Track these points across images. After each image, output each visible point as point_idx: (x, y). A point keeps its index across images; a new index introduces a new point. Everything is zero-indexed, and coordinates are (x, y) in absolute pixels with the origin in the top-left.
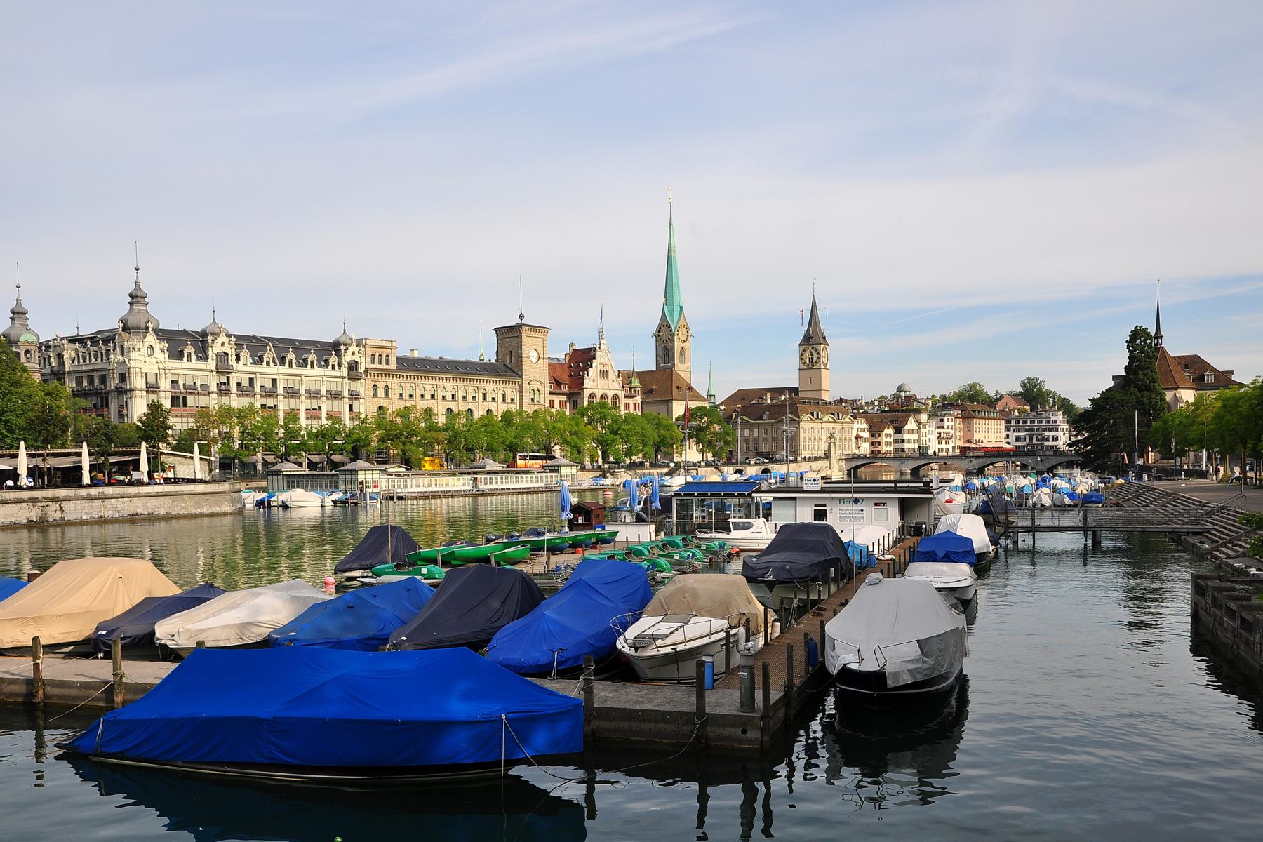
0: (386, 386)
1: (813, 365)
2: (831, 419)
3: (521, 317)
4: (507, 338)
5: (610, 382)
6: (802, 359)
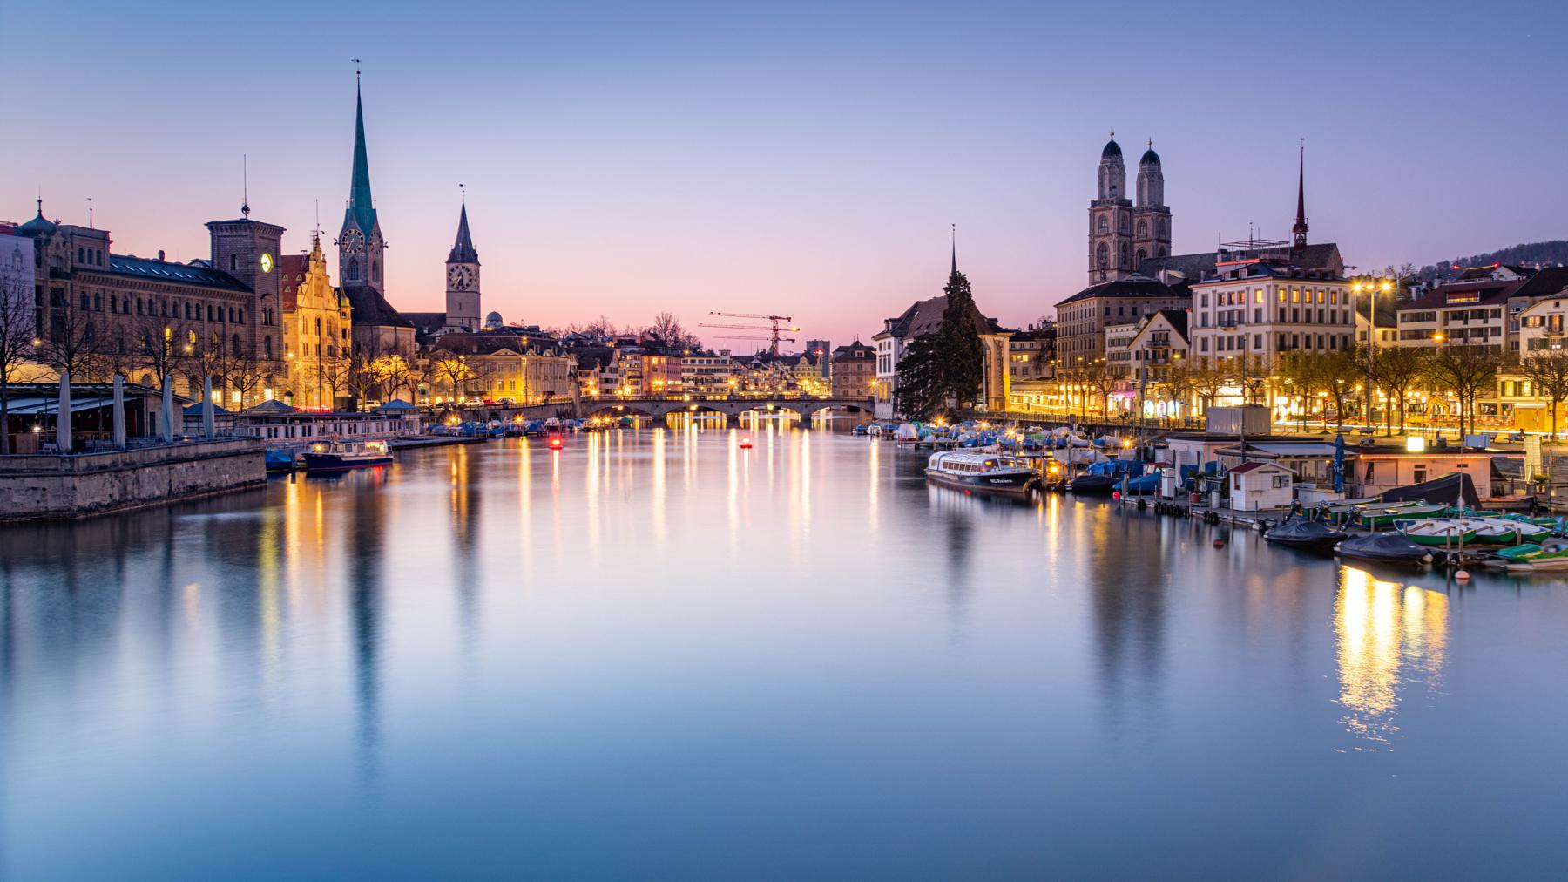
0: (97, 295)
1: (463, 288)
2: (548, 355)
3: (246, 209)
4: (228, 236)
5: (326, 302)
6: (450, 280)
